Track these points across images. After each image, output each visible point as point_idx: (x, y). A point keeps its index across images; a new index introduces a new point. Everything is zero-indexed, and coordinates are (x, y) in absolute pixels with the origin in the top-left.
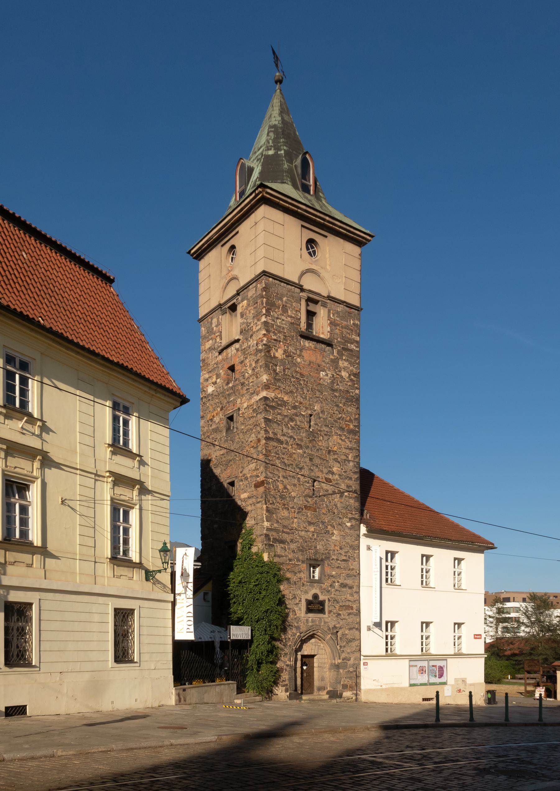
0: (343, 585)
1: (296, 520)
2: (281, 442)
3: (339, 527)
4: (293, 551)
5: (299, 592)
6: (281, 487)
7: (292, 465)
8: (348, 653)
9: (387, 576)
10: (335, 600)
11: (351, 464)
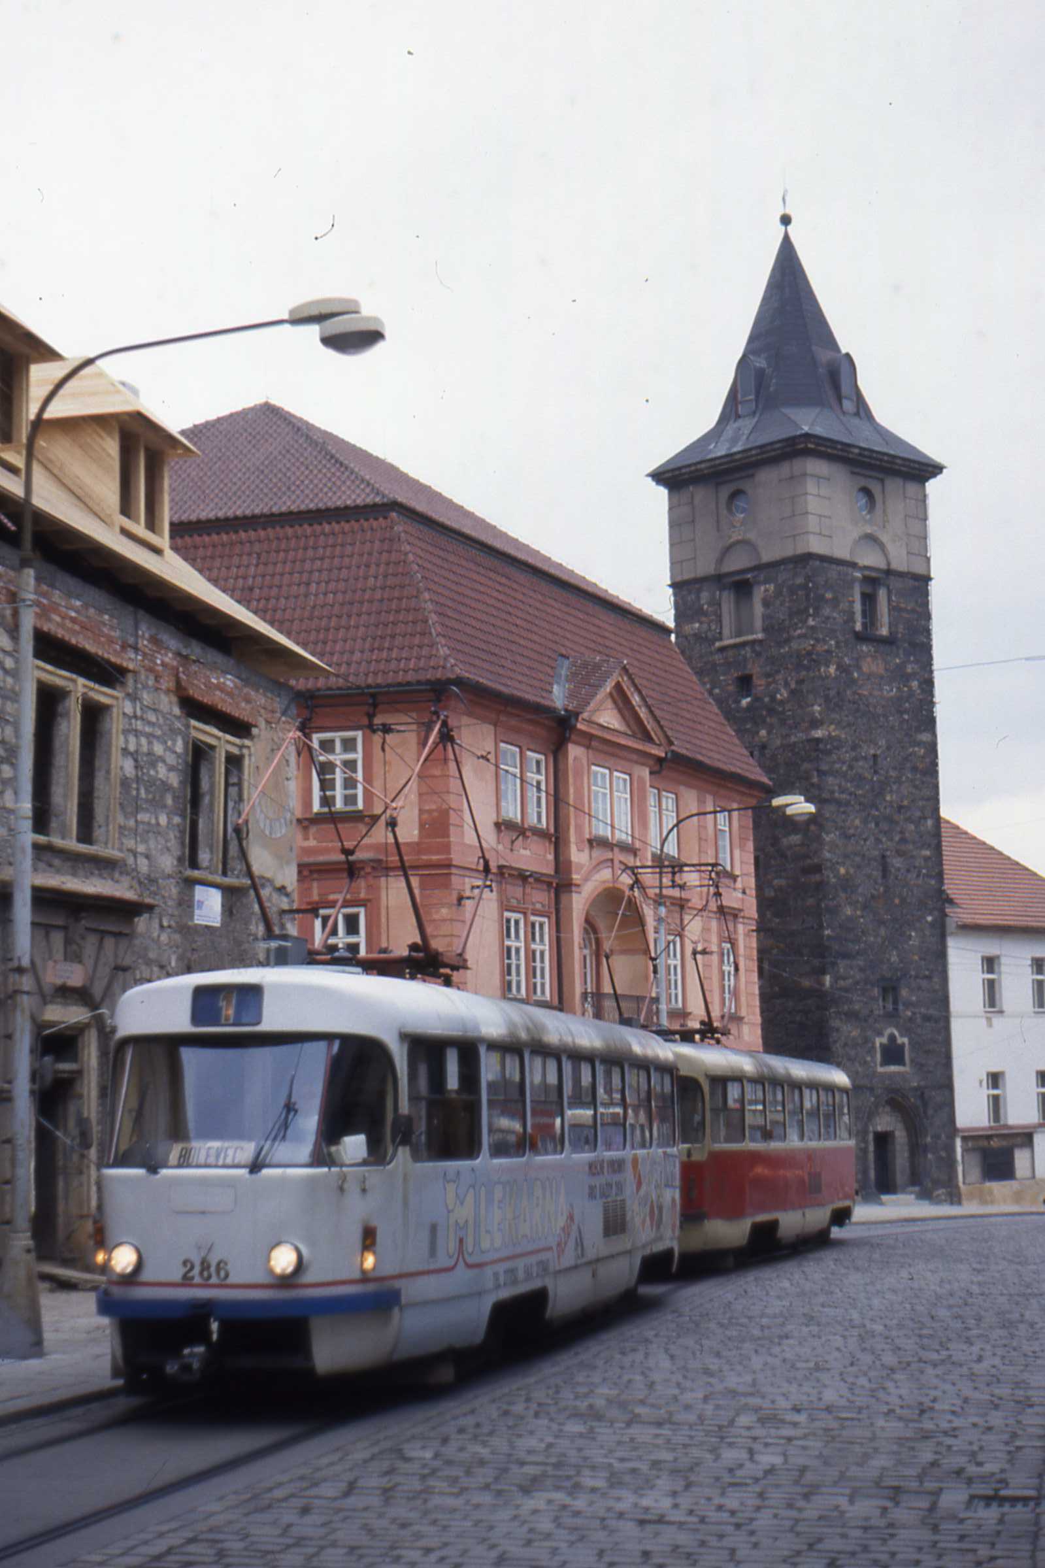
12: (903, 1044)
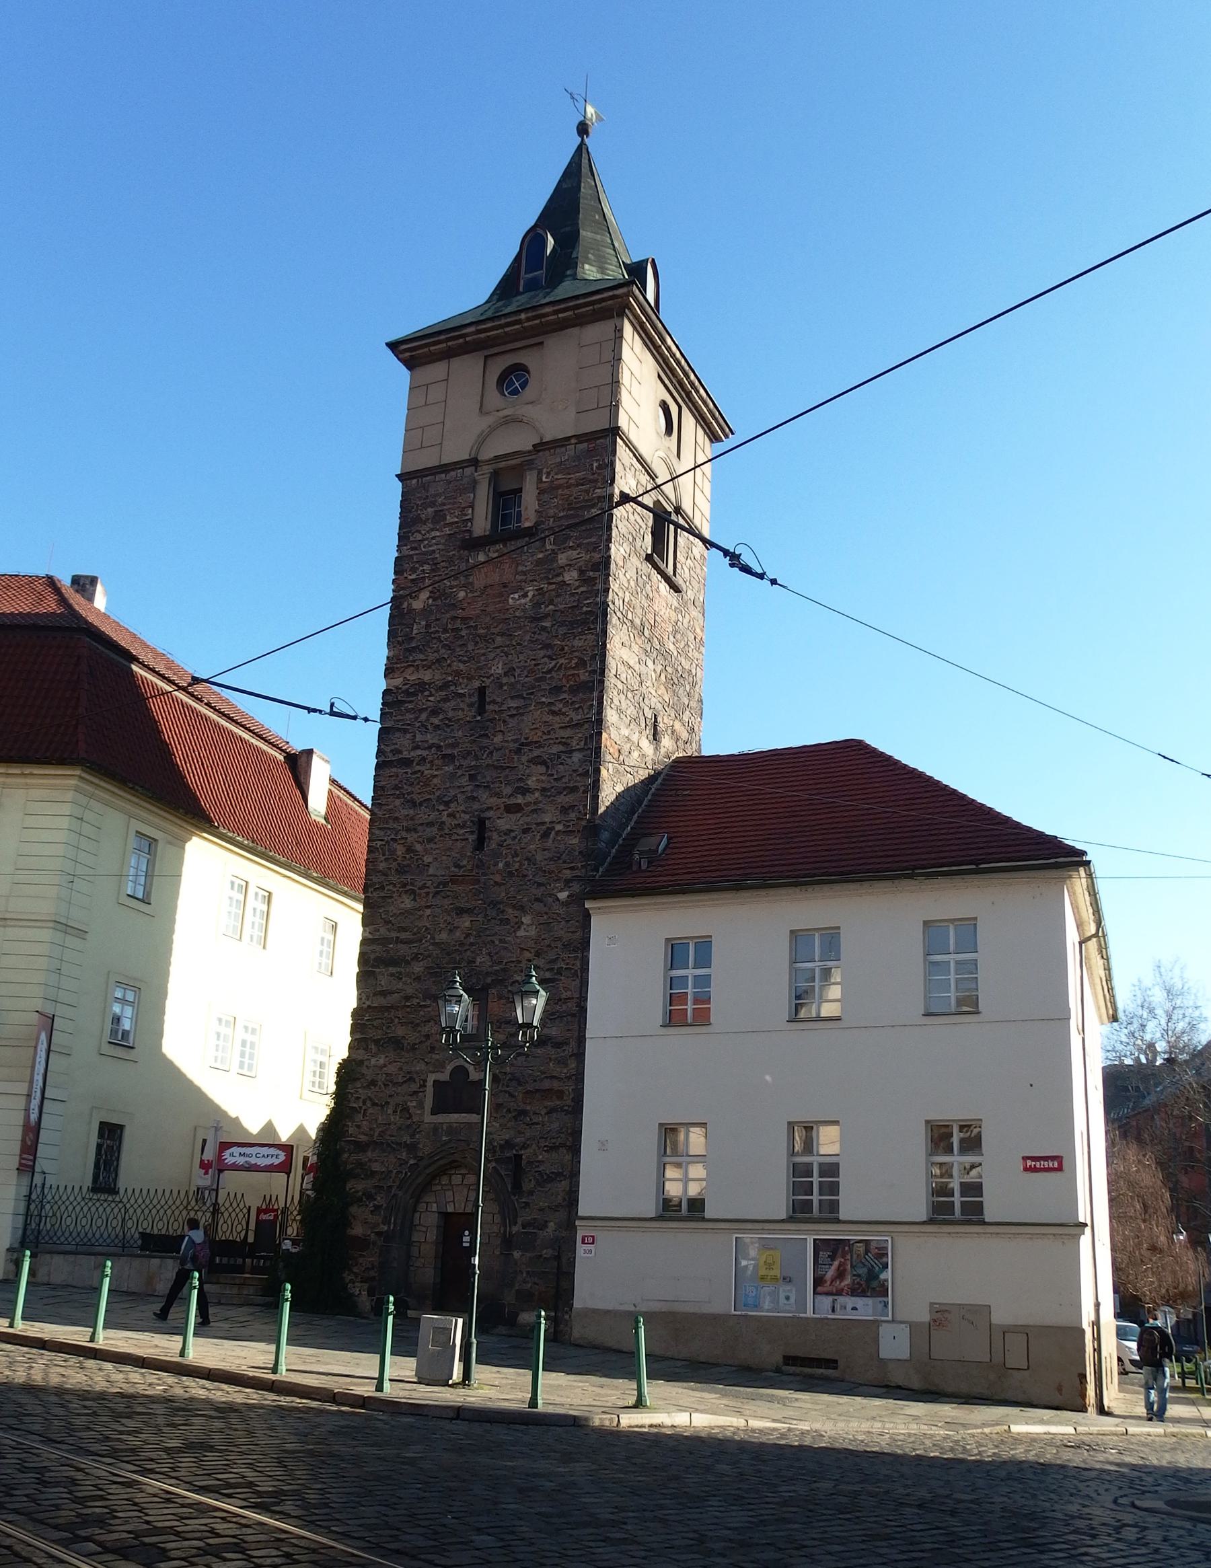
1: (428, 912)
2: (407, 762)
3: (538, 906)
4: (418, 979)
5: (421, 1066)
6: (400, 850)
7: (429, 799)
9: (684, 1010)
10: (514, 1078)
11: (577, 757)
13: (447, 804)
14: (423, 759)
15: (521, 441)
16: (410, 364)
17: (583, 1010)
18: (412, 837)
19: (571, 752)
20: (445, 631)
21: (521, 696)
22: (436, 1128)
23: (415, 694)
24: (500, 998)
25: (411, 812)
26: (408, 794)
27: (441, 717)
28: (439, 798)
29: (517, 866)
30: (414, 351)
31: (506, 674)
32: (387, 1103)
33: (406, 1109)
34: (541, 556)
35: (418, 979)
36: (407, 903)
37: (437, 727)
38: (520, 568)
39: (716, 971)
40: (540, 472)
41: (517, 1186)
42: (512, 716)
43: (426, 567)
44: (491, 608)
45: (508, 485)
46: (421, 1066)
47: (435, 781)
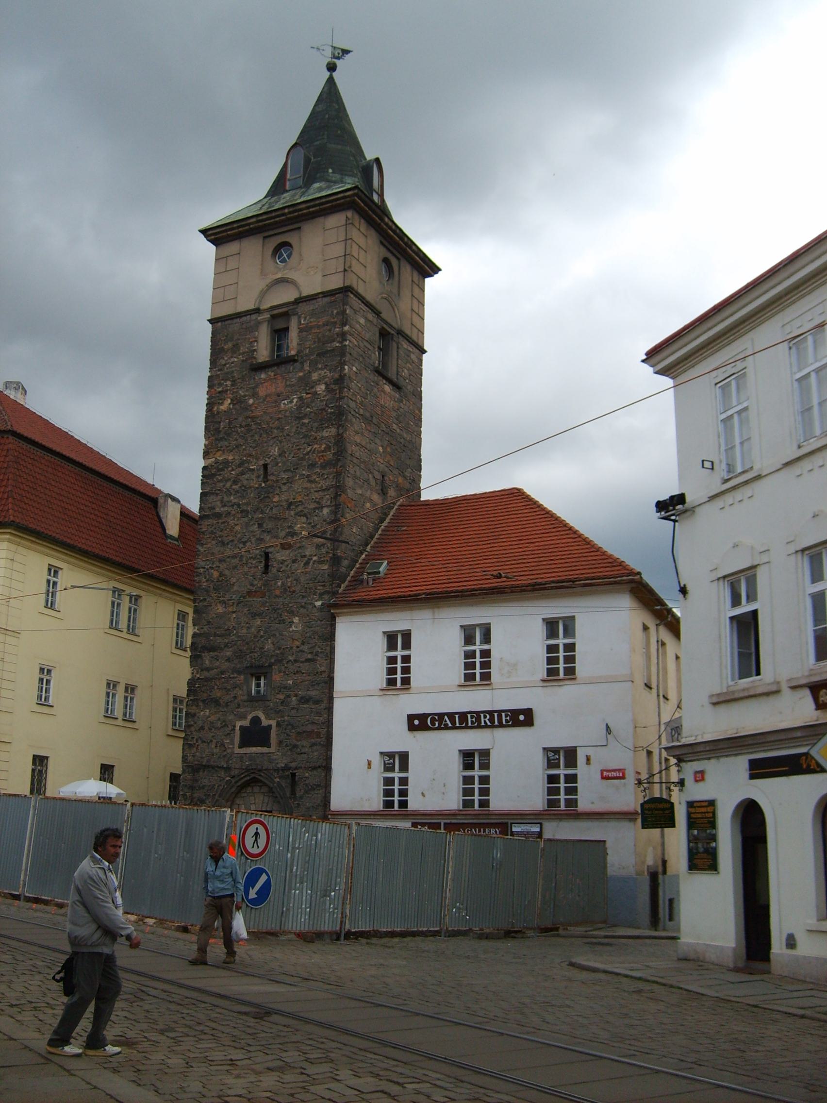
0: (305, 700)
1: (234, 615)
2: (218, 516)
3: (302, 611)
4: (228, 660)
5: (231, 717)
6: (216, 574)
7: (232, 541)
8: (308, 808)
10: (289, 724)
11: (326, 511)
12: (270, 726)
13: (244, 543)
14: (229, 514)
15: (286, 295)
16: (216, 242)
17: (331, 679)
18: (223, 566)
19: (322, 507)
20: (241, 426)
21: (289, 470)
22: (241, 757)
23: (222, 470)
24: (280, 672)
25: (222, 549)
26: (220, 537)
27: (239, 485)
28: (240, 539)
29: (289, 584)
30: (217, 235)
31: (280, 455)
32: (211, 741)
33: (223, 745)
34: (301, 374)
35: (228, 660)
36: (220, 609)
37: (237, 492)
38: (288, 383)
39: (415, 652)
40: (299, 317)
41: (293, 792)
42: (284, 484)
43: (229, 383)
44: (270, 410)
45: (280, 324)
46: (231, 717)
47: (238, 528)
